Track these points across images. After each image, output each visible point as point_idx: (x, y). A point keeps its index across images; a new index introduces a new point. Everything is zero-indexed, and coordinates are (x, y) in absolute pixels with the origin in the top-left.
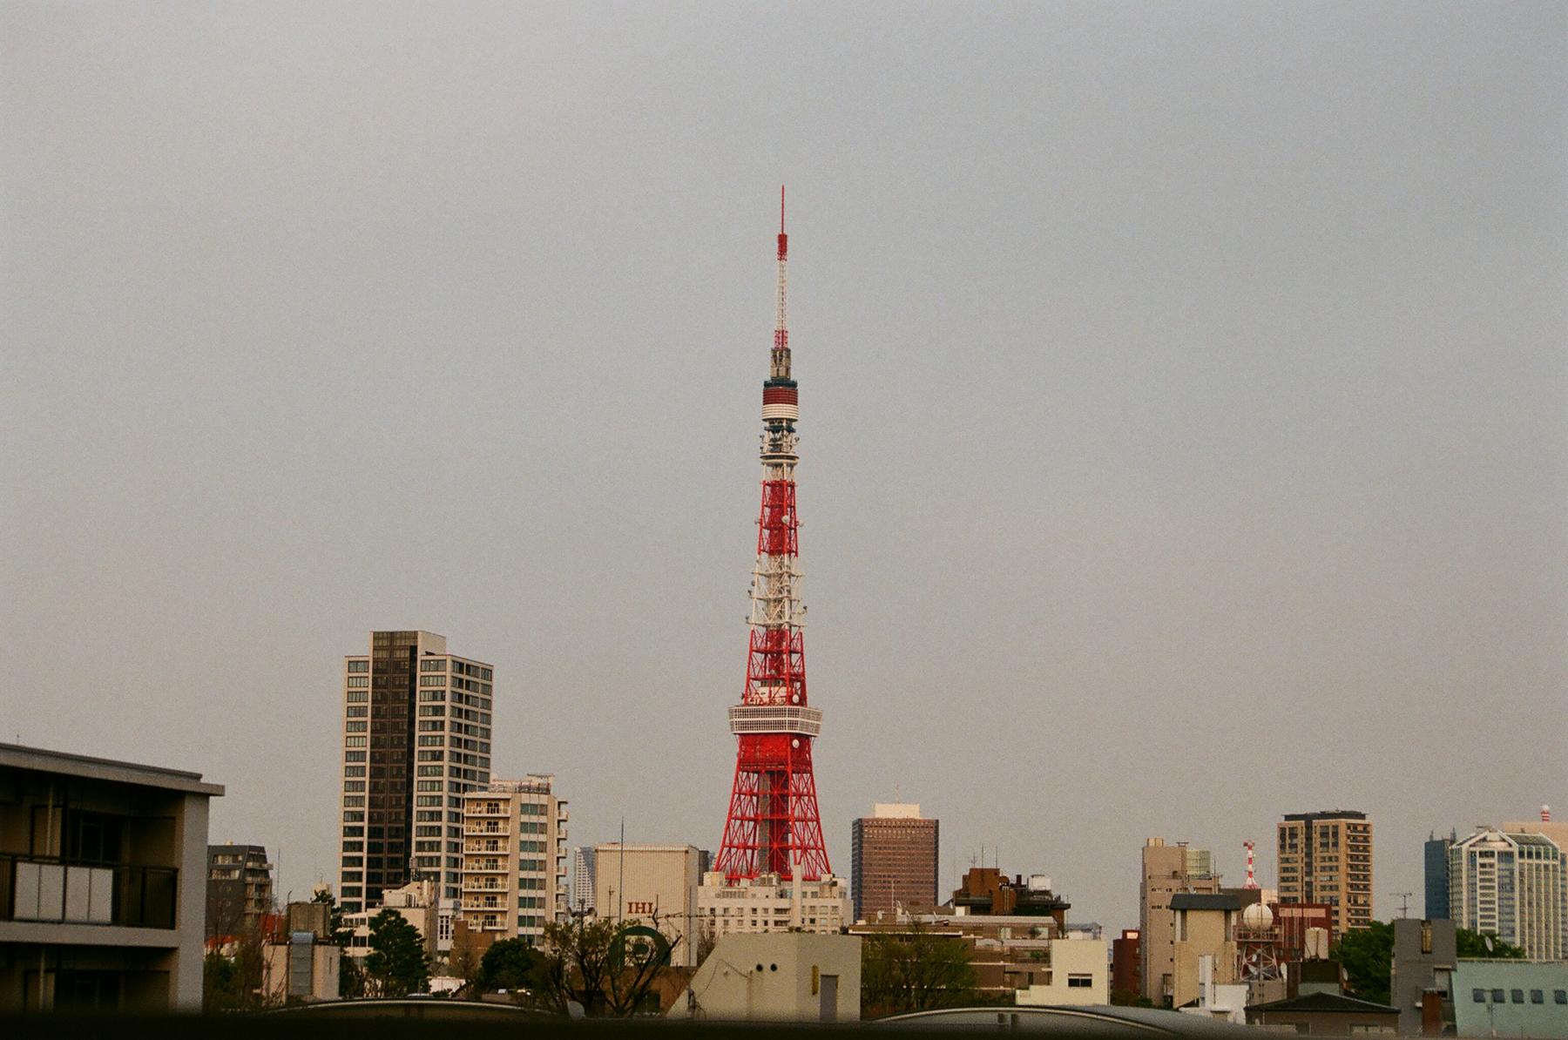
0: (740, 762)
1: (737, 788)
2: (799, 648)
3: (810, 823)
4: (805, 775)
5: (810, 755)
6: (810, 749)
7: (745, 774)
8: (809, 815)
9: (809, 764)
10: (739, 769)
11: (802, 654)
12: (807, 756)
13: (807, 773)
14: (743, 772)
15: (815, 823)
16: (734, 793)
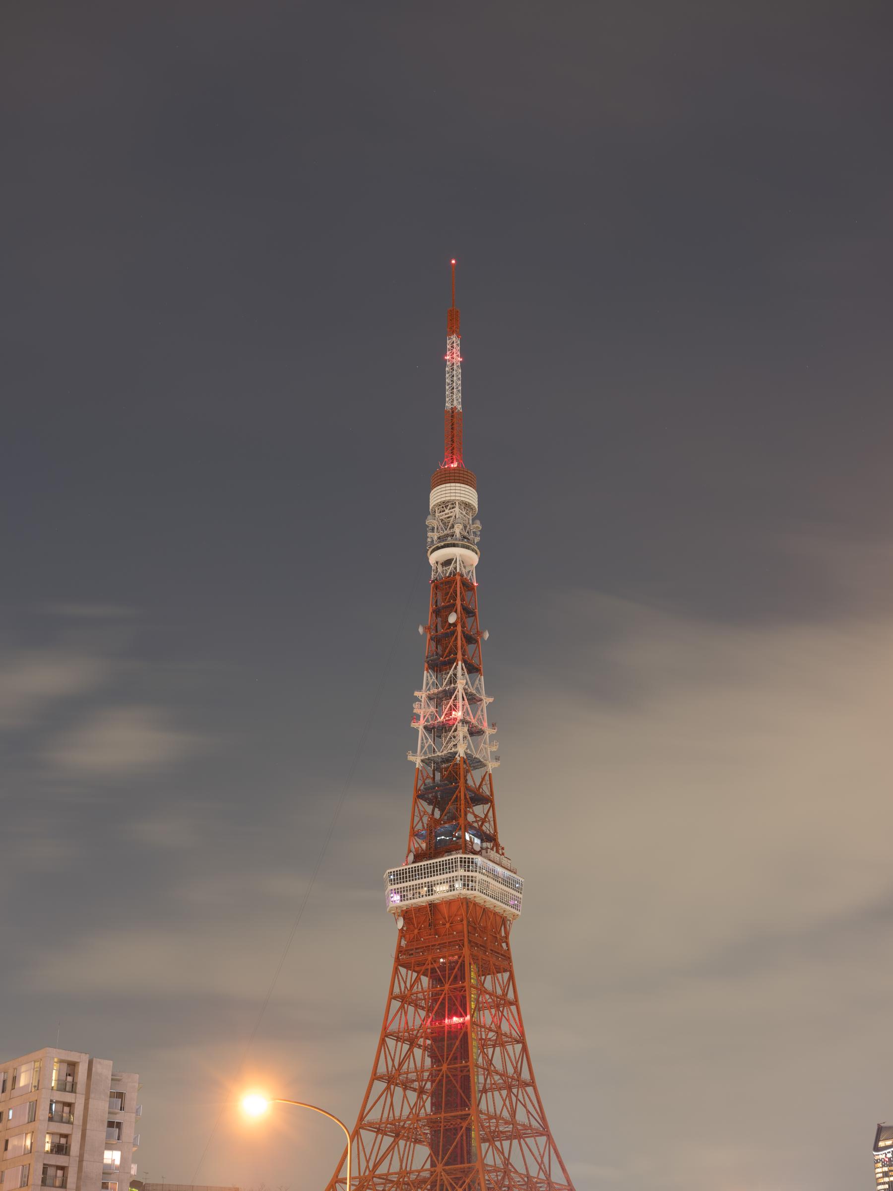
0: (400, 950)
1: (397, 990)
2: (486, 790)
3: (509, 1048)
4: (499, 975)
5: (507, 945)
6: (507, 934)
7: (410, 972)
8: (505, 1027)
9: (507, 957)
10: (399, 962)
11: (492, 802)
12: (504, 945)
13: (505, 971)
14: (407, 966)
15: (519, 1047)
16: (392, 997)
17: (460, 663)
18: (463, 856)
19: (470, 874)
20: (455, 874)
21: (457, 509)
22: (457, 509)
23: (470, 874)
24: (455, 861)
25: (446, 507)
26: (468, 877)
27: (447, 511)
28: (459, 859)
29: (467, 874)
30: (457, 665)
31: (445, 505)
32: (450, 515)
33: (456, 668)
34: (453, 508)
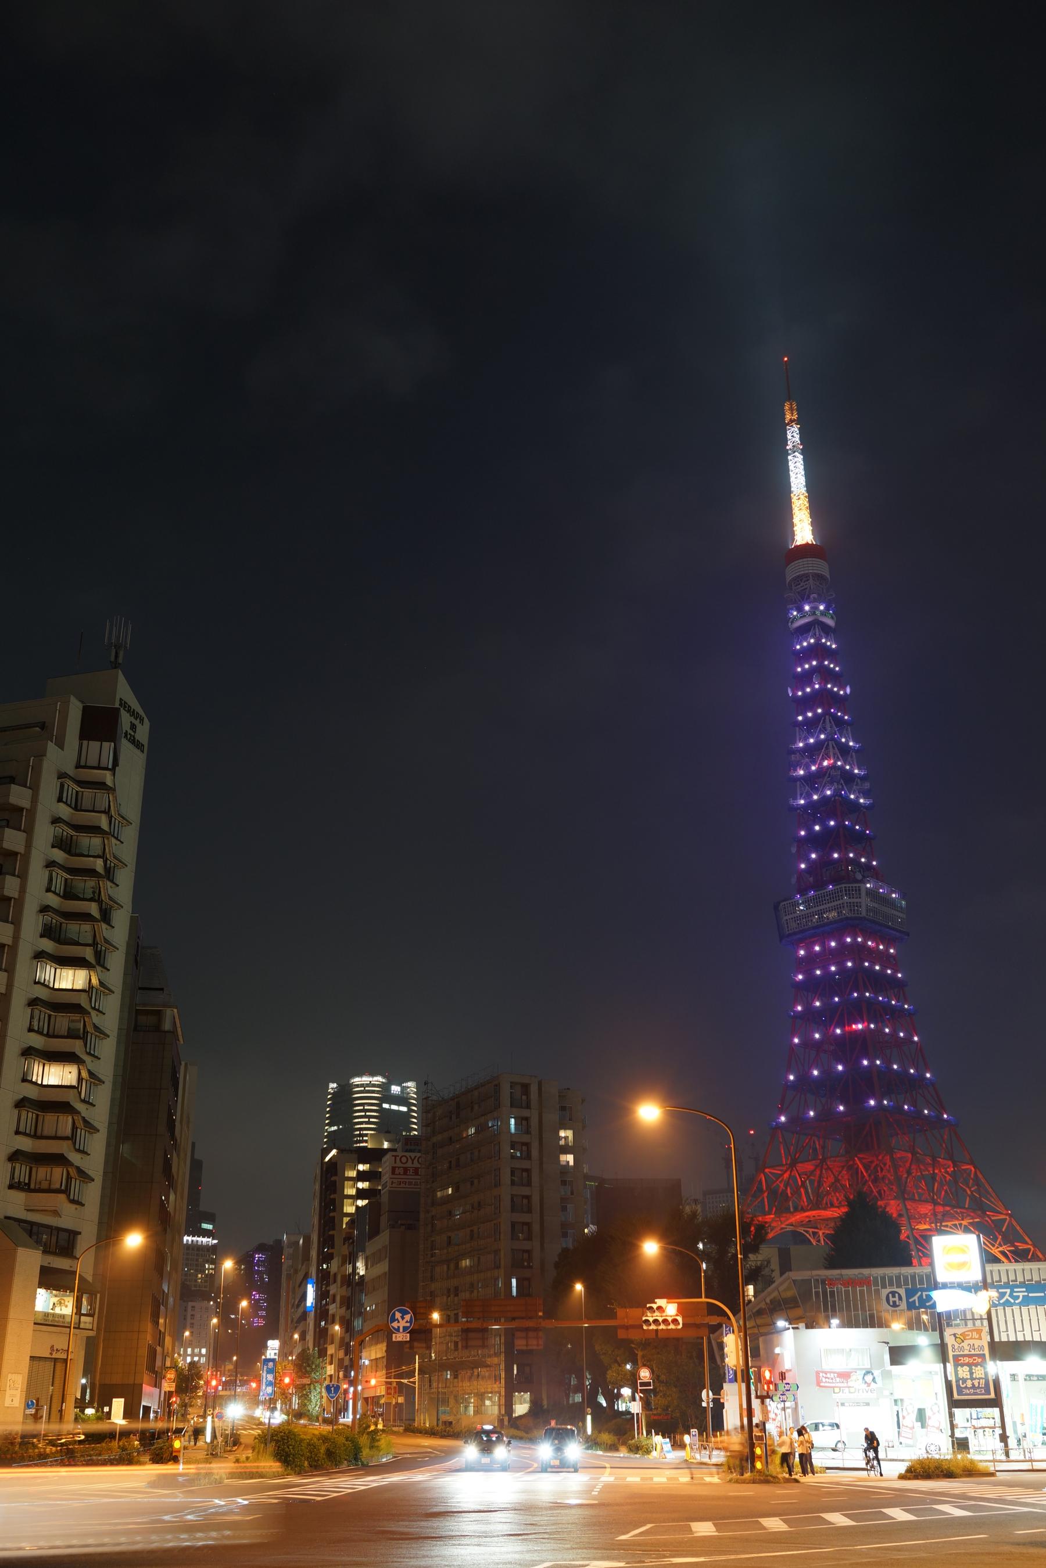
17: (827, 717)
18: (847, 885)
19: (855, 900)
20: (838, 902)
21: (811, 581)
22: (811, 581)
23: (855, 900)
24: (840, 891)
25: (801, 580)
26: (853, 903)
27: (802, 584)
28: (844, 889)
29: (852, 900)
30: (825, 719)
31: (799, 579)
32: (805, 587)
33: (824, 722)
34: (808, 580)
